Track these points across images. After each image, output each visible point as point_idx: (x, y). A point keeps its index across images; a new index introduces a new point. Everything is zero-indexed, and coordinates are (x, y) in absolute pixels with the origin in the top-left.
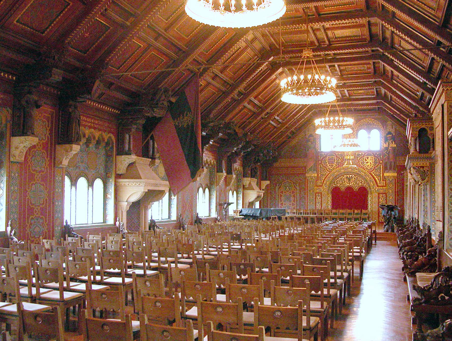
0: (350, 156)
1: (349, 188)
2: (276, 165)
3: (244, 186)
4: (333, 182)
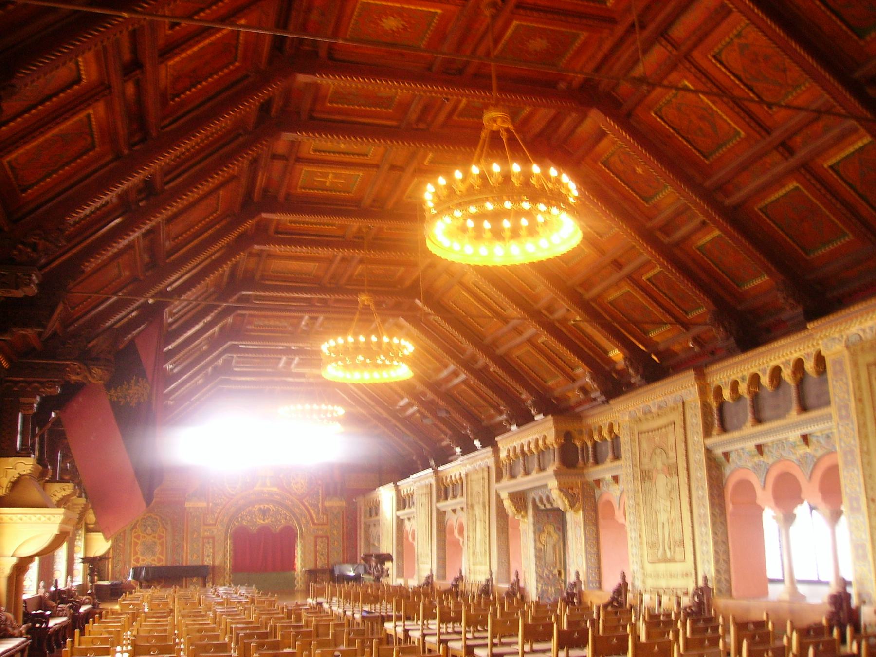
3: (86, 524)
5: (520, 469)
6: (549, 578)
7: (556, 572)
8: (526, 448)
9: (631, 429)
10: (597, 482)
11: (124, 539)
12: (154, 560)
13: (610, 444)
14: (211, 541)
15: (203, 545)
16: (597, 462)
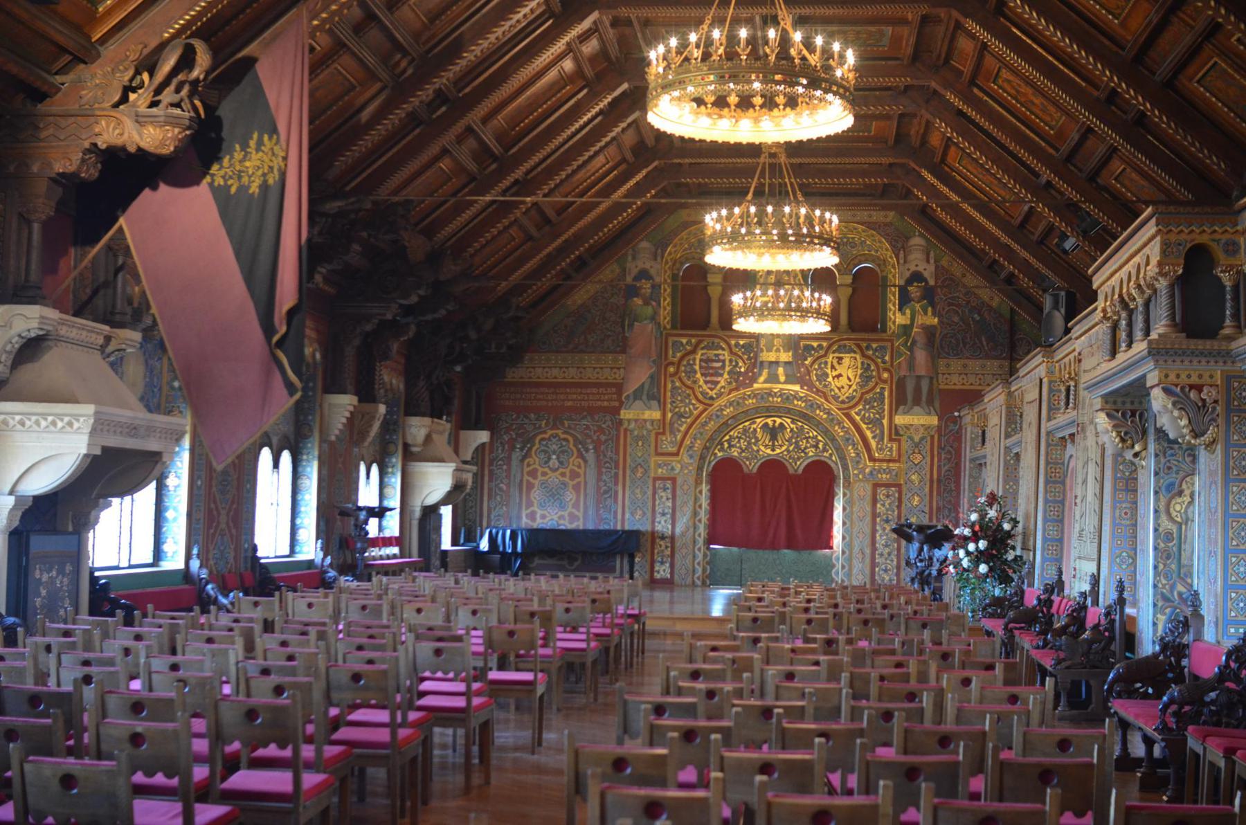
0: (778, 350)
1: (773, 466)
2: (515, 374)
4: (714, 440)
11: (508, 477)
12: (562, 517)
15: (654, 493)
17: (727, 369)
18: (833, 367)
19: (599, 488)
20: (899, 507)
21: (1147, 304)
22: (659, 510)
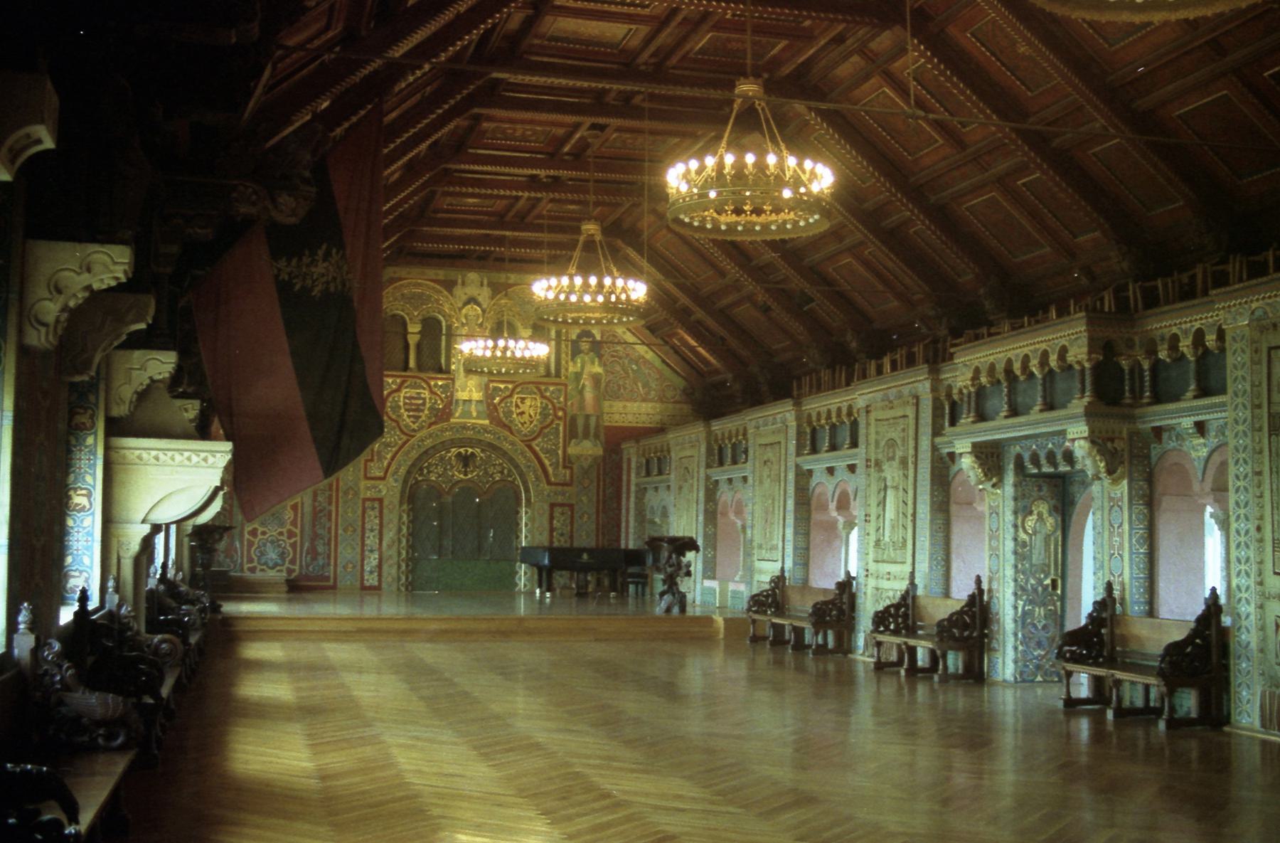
4: (417, 466)
5: (999, 403)
6: (1035, 590)
7: (1048, 582)
8: (1017, 367)
9: (1253, 341)
10: (1158, 432)
13: (1193, 366)
14: (376, 505)
16: (1157, 399)
17: (428, 405)
18: (517, 406)
19: (314, 508)
20: (572, 523)
21: (1044, 379)
22: (368, 526)
